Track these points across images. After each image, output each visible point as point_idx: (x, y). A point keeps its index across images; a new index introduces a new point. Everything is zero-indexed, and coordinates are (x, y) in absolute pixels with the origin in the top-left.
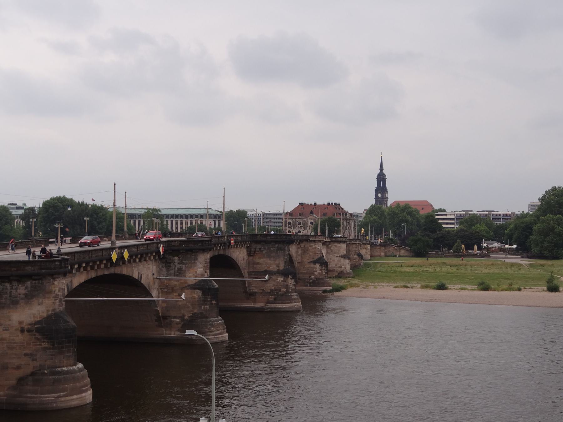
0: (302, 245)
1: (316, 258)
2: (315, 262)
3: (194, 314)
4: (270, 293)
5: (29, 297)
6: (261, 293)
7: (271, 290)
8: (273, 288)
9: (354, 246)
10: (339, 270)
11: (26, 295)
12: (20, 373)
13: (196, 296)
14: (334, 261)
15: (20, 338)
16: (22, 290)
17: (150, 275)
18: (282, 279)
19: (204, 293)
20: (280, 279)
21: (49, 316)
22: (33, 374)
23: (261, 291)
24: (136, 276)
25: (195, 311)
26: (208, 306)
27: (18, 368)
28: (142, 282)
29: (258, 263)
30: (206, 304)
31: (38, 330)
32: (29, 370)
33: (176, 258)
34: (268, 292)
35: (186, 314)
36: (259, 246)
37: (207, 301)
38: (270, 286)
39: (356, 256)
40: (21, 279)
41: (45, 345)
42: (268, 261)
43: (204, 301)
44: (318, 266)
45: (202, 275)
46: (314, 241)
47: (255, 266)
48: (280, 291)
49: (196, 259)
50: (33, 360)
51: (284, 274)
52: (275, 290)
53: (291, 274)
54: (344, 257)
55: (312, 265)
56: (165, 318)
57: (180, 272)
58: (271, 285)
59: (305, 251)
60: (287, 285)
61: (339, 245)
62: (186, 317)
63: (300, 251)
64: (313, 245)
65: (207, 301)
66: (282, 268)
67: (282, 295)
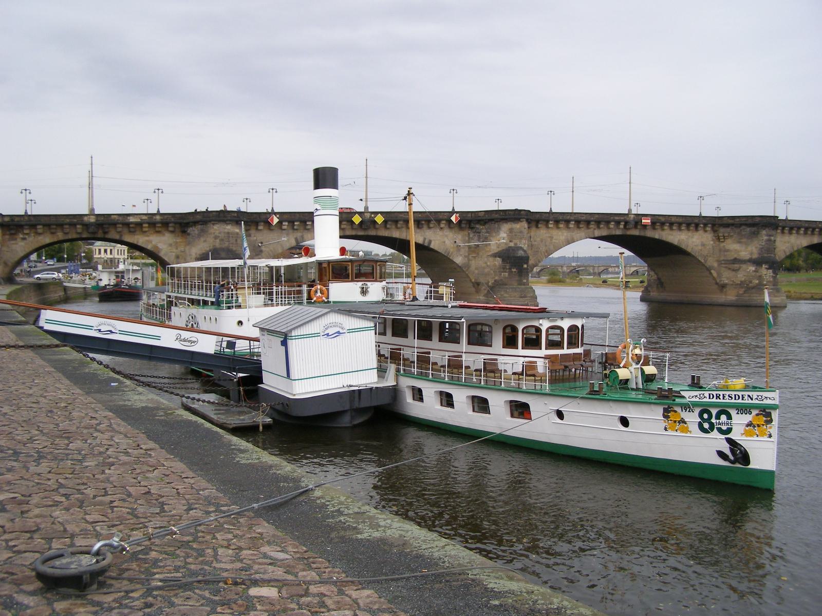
3: (495, 281)
4: (740, 284)
5: (199, 236)
6: (732, 285)
7: (741, 282)
8: (743, 279)
18: (754, 269)
19: (503, 260)
20: (752, 268)
23: (731, 283)
25: (497, 278)
26: (507, 274)
28: (432, 246)
30: (505, 272)
34: (738, 284)
35: (490, 280)
36: (728, 230)
37: (507, 269)
38: (741, 276)
43: (504, 269)
45: (506, 244)
47: (726, 253)
48: (751, 282)
49: (499, 228)
51: (758, 262)
52: (745, 281)
53: (766, 263)
56: (478, 284)
58: (741, 275)
60: (760, 276)
65: (507, 269)
66: (755, 256)
67: (753, 288)
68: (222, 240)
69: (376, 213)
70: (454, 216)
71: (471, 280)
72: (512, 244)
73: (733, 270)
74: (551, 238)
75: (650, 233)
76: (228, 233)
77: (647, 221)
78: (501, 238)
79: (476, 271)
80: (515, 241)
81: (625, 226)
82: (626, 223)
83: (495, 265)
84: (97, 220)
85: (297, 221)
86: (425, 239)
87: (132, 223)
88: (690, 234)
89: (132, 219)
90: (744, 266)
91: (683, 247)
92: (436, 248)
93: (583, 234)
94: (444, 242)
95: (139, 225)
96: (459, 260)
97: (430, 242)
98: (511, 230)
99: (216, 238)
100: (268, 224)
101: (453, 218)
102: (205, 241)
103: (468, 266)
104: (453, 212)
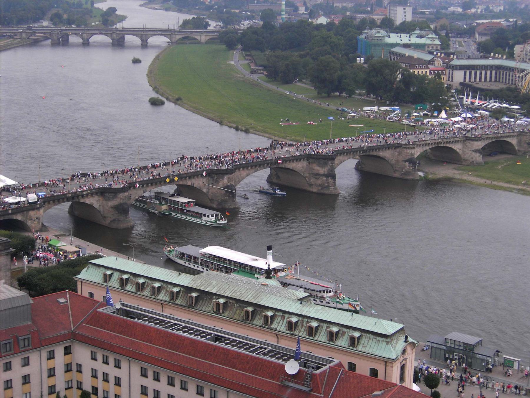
0: (398, 150)
1: (407, 158)
2: (406, 161)
9: (525, 137)
10: (471, 160)
12: (111, 219)
14: (468, 153)
15: (111, 209)
16: (111, 196)
17: (201, 183)
24: (189, 183)
29: (314, 169)
38: (319, 182)
39: (526, 145)
42: (318, 168)
44: (407, 164)
46: (405, 148)
54: (476, 151)
55: (404, 163)
59: (400, 154)
61: (472, 143)
63: (397, 153)
64: (405, 150)
66: (326, 173)
72: (229, 184)
73: (316, 178)
74: (241, 174)
75: (280, 166)
78: (225, 181)
89: (84, 193)
90: (321, 177)
93: (253, 171)
95: (87, 195)
96: (205, 190)
98: (229, 178)
99: (121, 199)
100: (135, 187)
101: (204, 174)
103: (208, 192)
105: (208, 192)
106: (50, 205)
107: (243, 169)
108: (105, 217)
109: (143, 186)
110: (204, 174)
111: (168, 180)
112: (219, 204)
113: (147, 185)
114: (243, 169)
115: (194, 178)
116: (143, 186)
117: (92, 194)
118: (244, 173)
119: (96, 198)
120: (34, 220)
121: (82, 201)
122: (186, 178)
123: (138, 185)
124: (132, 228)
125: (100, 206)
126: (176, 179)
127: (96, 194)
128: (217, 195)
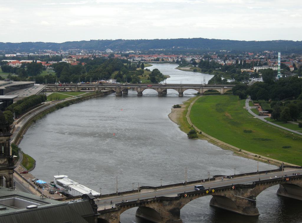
3: (246, 207)
5: (169, 204)
11: (168, 204)
12: (167, 220)
13: (246, 201)
15: (167, 213)
16: (167, 203)
17: (231, 194)
21: (173, 209)
22: (169, 220)
24: (223, 195)
25: (246, 206)
27: (167, 218)
28: (226, 196)
31: (170, 211)
32: (168, 219)
33: (241, 189)
40: (167, 201)
41: (171, 215)
45: (249, 195)
49: (247, 190)
50: (169, 217)
56: (239, 207)
57: (243, 194)
62: (244, 207)
68: (176, 205)
69: (212, 189)
70: (233, 187)
71: (236, 205)
72: (251, 195)
74: (259, 188)
75: (288, 183)
76: (178, 203)
77: (288, 179)
78: (249, 192)
79: (238, 203)
80: (252, 194)
81: (281, 182)
82: (282, 180)
83: (246, 202)
84: (140, 202)
85: (191, 195)
86: (224, 195)
87: (149, 201)
88: (300, 181)
89: (149, 200)
91: (298, 185)
92: (227, 197)
93: (268, 186)
94: (229, 194)
95: (151, 202)
96: (233, 200)
97: (226, 195)
99: (175, 205)
100: (184, 197)
101: (233, 188)
102: (171, 206)
103: (236, 201)
104: (232, 186)
105: (236, 201)
106: (125, 209)
107: (261, 185)
108: (163, 218)
109: (190, 196)
110: (233, 188)
111: (207, 192)
112: (244, 210)
113: (193, 195)
114: (261, 185)
115: (226, 191)
116: (190, 196)
117: (154, 201)
118: (261, 187)
119: (157, 204)
120: (114, 219)
121: (147, 206)
122: (220, 190)
123: (186, 195)
124: (259, 215)
125: (159, 210)
126: (213, 191)
127: (157, 201)
128: (242, 203)
